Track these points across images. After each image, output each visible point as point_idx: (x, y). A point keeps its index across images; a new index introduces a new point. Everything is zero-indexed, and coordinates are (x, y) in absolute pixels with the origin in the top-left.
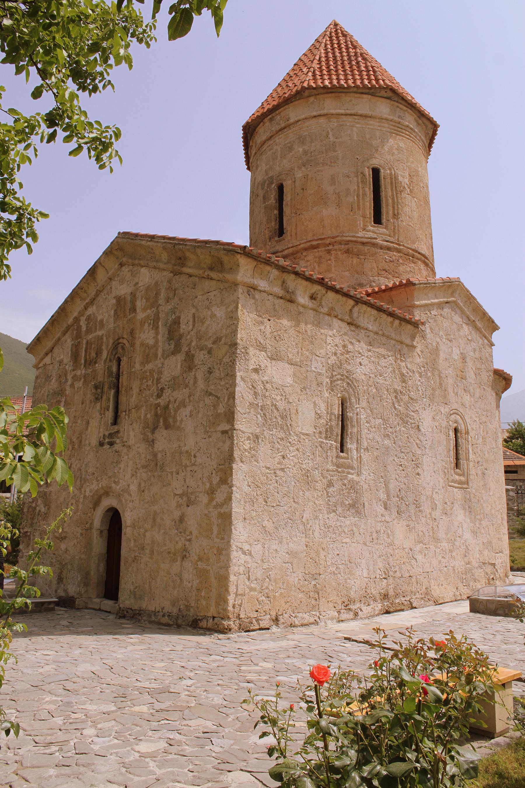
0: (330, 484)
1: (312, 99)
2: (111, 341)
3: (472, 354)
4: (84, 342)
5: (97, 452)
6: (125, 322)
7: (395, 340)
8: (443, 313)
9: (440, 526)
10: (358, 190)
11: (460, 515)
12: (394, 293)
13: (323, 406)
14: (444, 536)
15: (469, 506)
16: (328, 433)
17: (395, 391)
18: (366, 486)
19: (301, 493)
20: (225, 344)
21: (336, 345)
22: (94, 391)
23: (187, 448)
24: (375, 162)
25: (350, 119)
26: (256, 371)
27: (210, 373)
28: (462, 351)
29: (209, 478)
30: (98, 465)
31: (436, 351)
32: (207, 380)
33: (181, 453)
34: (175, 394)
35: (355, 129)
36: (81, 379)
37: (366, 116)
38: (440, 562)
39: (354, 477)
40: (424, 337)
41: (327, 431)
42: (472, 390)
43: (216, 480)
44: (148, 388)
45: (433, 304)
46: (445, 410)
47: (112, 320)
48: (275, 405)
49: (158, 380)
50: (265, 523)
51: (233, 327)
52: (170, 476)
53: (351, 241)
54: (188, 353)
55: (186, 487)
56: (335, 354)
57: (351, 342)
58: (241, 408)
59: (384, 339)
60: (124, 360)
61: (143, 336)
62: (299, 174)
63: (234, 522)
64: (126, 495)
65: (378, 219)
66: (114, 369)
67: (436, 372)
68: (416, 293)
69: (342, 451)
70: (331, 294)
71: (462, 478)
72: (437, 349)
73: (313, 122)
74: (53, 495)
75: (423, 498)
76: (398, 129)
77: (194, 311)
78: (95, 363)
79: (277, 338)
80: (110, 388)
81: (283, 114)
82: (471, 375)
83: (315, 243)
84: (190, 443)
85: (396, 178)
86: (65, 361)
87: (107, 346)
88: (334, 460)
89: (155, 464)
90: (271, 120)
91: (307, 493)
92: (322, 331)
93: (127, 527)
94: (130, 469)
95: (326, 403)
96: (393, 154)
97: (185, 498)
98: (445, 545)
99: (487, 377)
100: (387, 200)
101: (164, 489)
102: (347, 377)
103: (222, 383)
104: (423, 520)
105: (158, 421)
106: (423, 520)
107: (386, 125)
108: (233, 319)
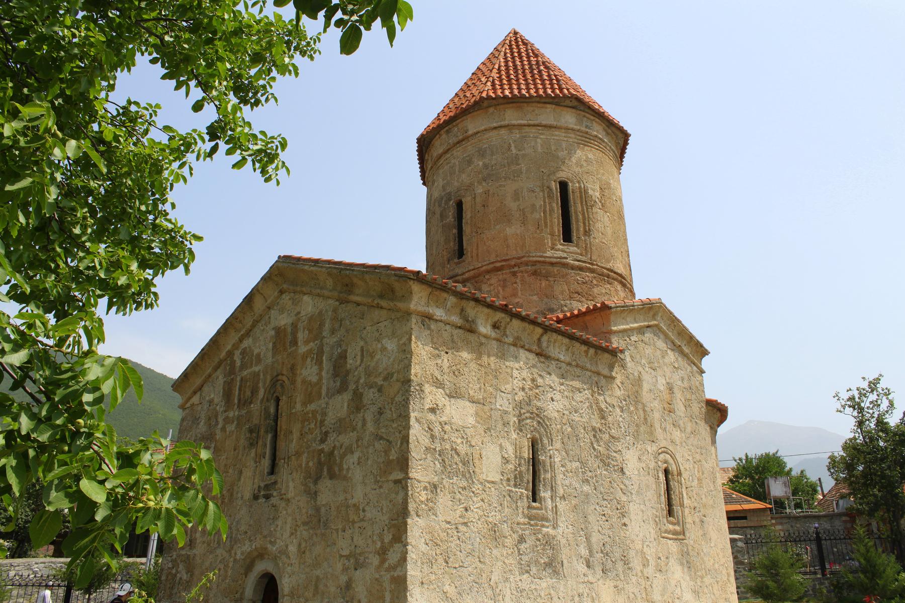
0: (522, 540)
1: (491, 110)
2: (269, 378)
3: (679, 383)
4: (238, 379)
5: (251, 506)
6: (285, 356)
7: (591, 371)
8: (644, 339)
9: (654, 586)
10: (545, 206)
11: (677, 572)
12: (587, 318)
13: (511, 450)
14: (660, 598)
15: (687, 561)
16: (517, 480)
17: (594, 429)
18: (563, 541)
19: (488, 551)
20: (397, 381)
21: (524, 379)
22: (248, 435)
23: (355, 501)
24: (562, 175)
25: (533, 130)
26: (433, 410)
27: (380, 413)
29: (381, 536)
30: (252, 522)
31: (638, 381)
32: (377, 422)
33: (348, 507)
34: (341, 438)
35: (539, 140)
36: (233, 422)
37: (550, 127)
39: (550, 531)
40: (623, 366)
41: (516, 478)
42: (682, 425)
43: (388, 538)
44: (311, 431)
45: (632, 330)
46: (652, 448)
47: (270, 353)
48: (456, 450)
49: (322, 422)
50: (447, 588)
51: (406, 361)
52: (335, 535)
53: (539, 262)
54: (356, 392)
55: (353, 547)
56: (523, 389)
57: (540, 375)
58: (416, 453)
59: (578, 371)
60: (284, 399)
61: (305, 372)
62: (479, 190)
63: (410, 587)
64: (283, 557)
65: (567, 237)
66: (272, 410)
67: (640, 406)
68: (612, 318)
69: (534, 500)
70: (516, 323)
71: (677, 528)
72: (640, 379)
73: (494, 133)
74: (197, 558)
75: (632, 553)
76: (586, 139)
77: (362, 343)
78: (251, 403)
79: (456, 373)
80: (267, 432)
81: (460, 126)
82: (680, 407)
83: (498, 265)
84: (358, 495)
85: (586, 191)
86: (216, 401)
87: (265, 384)
88: (526, 511)
89: (317, 521)
90: (448, 132)
91: (495, 552)
92: (507, 364)
93: (284, 596)
94: (288, 526)
96: (581, 166)
97: (352, 561)
99: (698, 409)
100: (577, 216)
101: (328, 550)
102: (537, 415)
103: (395, 425)
104: (634, 579)
105: (322, 470)
106: (634, 579)
107: (573, 136)
108: (406, 352)
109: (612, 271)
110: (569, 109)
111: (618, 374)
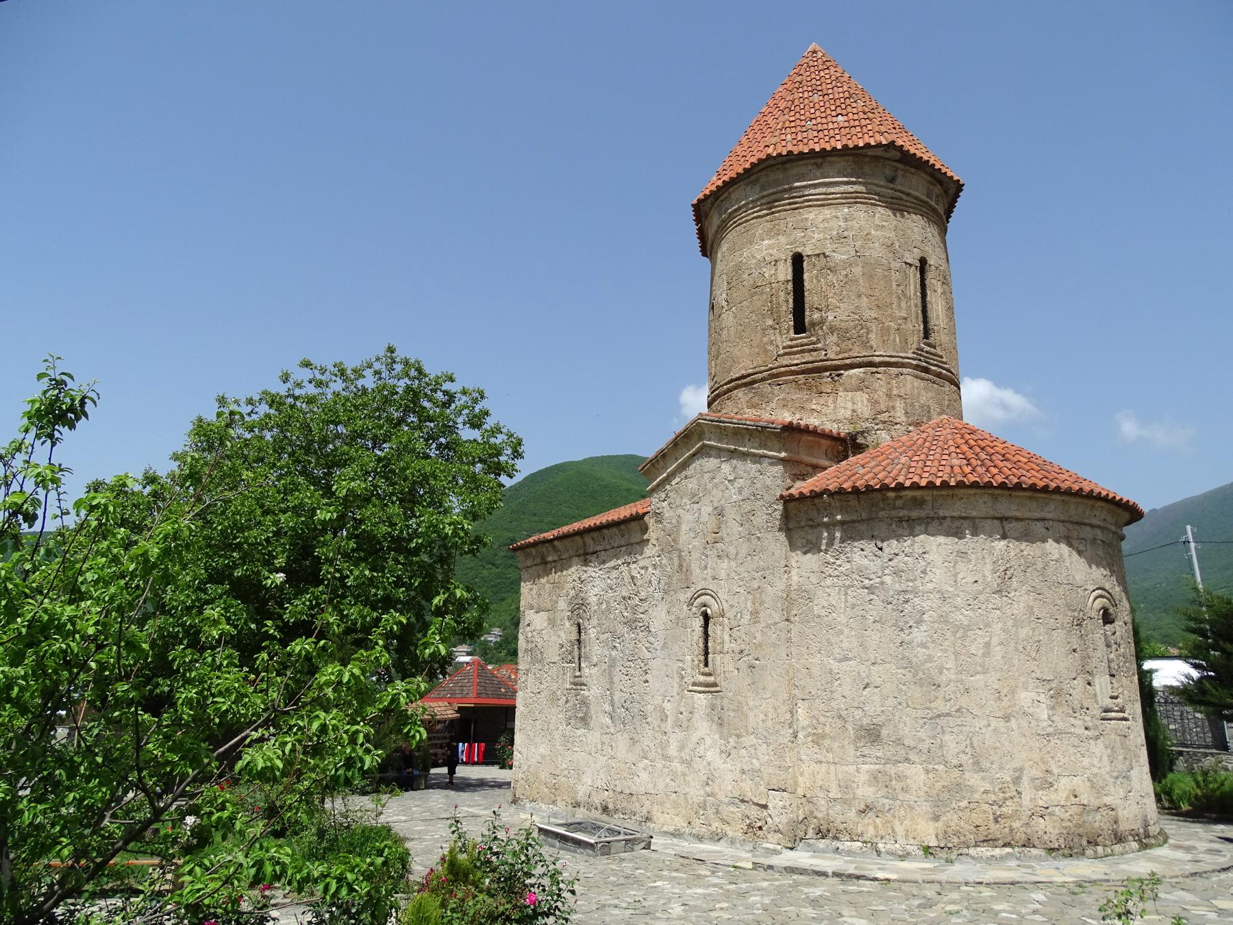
0: (567, 702)
11: (702, 727)
38: (667, 785)
39: (586, 693)
98: (678, 766)
111: (653, 534)
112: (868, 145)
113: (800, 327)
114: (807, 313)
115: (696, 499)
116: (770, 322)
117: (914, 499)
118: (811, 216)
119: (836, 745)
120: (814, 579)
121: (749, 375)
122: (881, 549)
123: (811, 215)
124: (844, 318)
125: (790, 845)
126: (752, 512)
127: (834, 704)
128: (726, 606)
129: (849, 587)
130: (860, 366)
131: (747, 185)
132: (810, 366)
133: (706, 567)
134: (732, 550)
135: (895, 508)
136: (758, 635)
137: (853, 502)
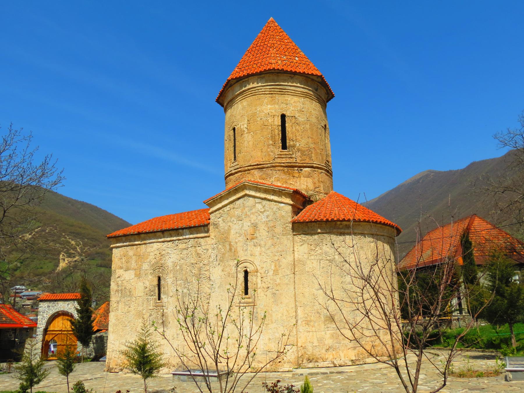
0: (151, 315)
16: (150, 293)
28: (252, 222)
71: (250, 300)
95: (151, 281)
109: (251, 166)
110: (235, 85)
112: (312, 74)
113: (284, 147)
114: (288, 141)
115: (240, 219)
116: (271, 142)
117: (346, 225)
118: (289, 99)
119: (316, 324)
120: (306, 256)
121: (261, 164)
122: (333, 245)
123: (289, 98)
124: (303, 146)
125: (296, 367)
126: (274, 227)
127: (315, 307)
128: (259, 268)
129: (321, 260)
130: (309, 167)
131: (258, 78)
132: (289, 164)
133: (246, 250)
134: (262, 243)
135: (339, 228)
136: (278, 281)
137: (324, 225)
